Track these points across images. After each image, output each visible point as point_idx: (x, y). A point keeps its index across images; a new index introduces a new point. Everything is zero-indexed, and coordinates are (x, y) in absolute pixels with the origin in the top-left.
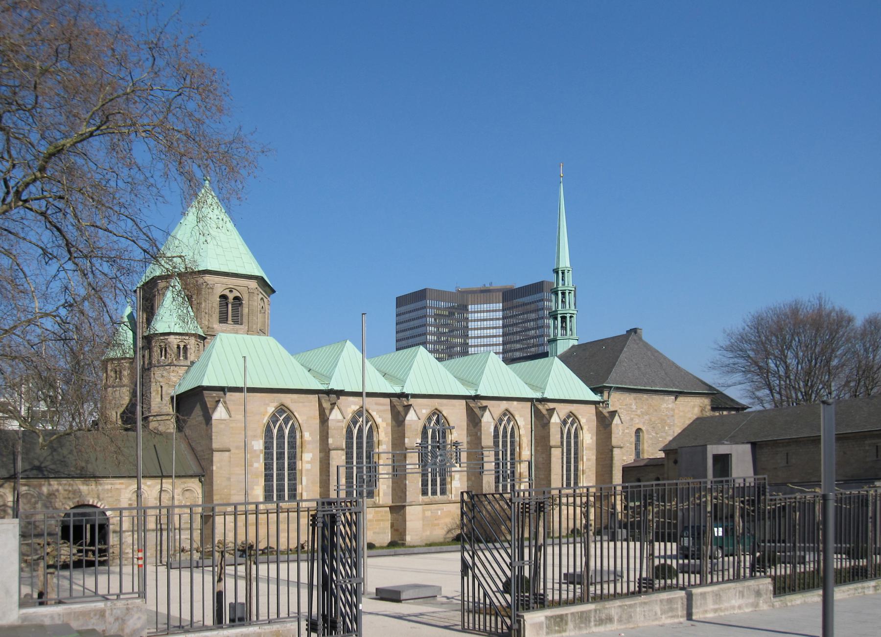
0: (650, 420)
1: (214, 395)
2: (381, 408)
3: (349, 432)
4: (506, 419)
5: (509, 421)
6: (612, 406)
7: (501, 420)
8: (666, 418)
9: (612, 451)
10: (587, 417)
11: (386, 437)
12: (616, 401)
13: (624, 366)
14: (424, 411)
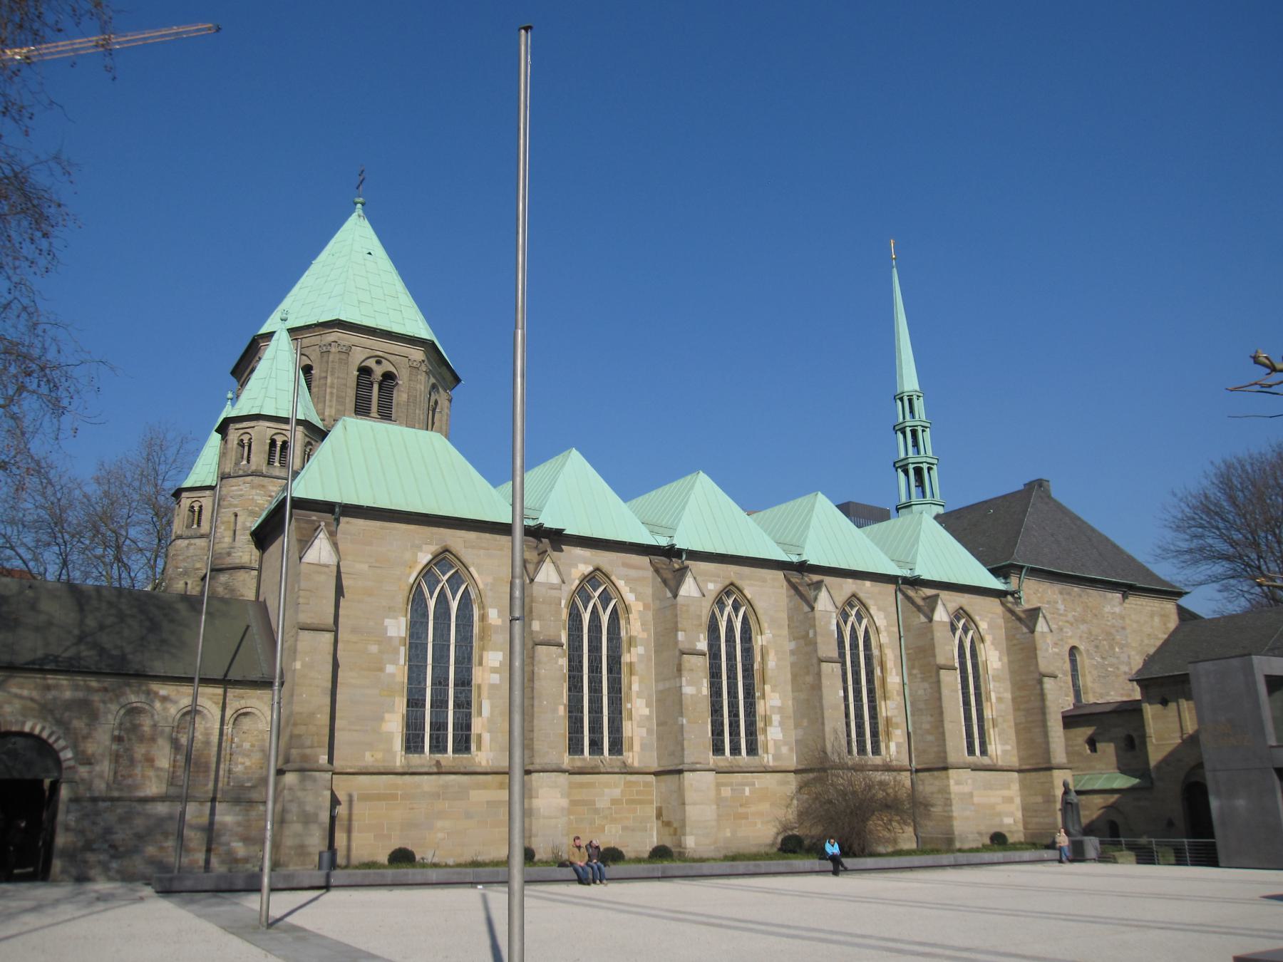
0: (1090, 633)
1: (314, 518)
2: (633, 573)
3: (575, 617)
4: (854, 612)
5: (859, 617)
6: (1028, 601)
7: (845, 616)
8: (1113, 631)
9: (1041, 683)
10: (988, 615)
11: (643, 630)
12: (1033, 592)
13: (1034, 536)
14: (711, 586)
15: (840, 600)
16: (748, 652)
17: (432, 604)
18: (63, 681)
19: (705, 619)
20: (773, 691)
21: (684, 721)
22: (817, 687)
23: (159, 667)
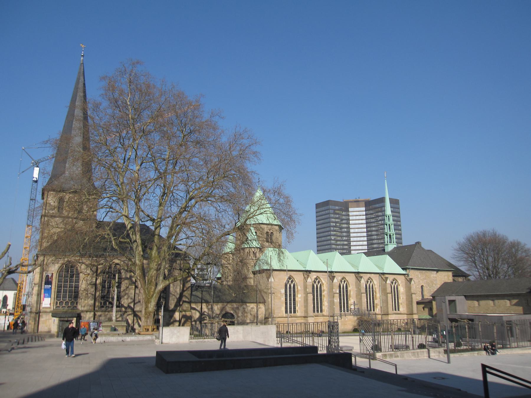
4: (369, 281)
7: (368, 282)
14: (339, 278)
15: (366, 280)
16: (347, 291)
17: (292, 286)
18: (235, 304)
19: (338, 285)
20: (352, 299)
21: (335, 307)
22: (361, 299)
23: (249, 301)
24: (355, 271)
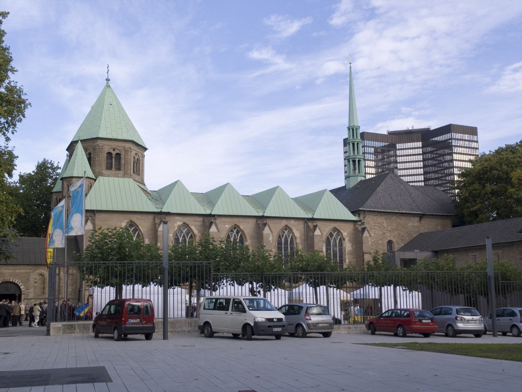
0: (400, 234)
24: (257, 214)
